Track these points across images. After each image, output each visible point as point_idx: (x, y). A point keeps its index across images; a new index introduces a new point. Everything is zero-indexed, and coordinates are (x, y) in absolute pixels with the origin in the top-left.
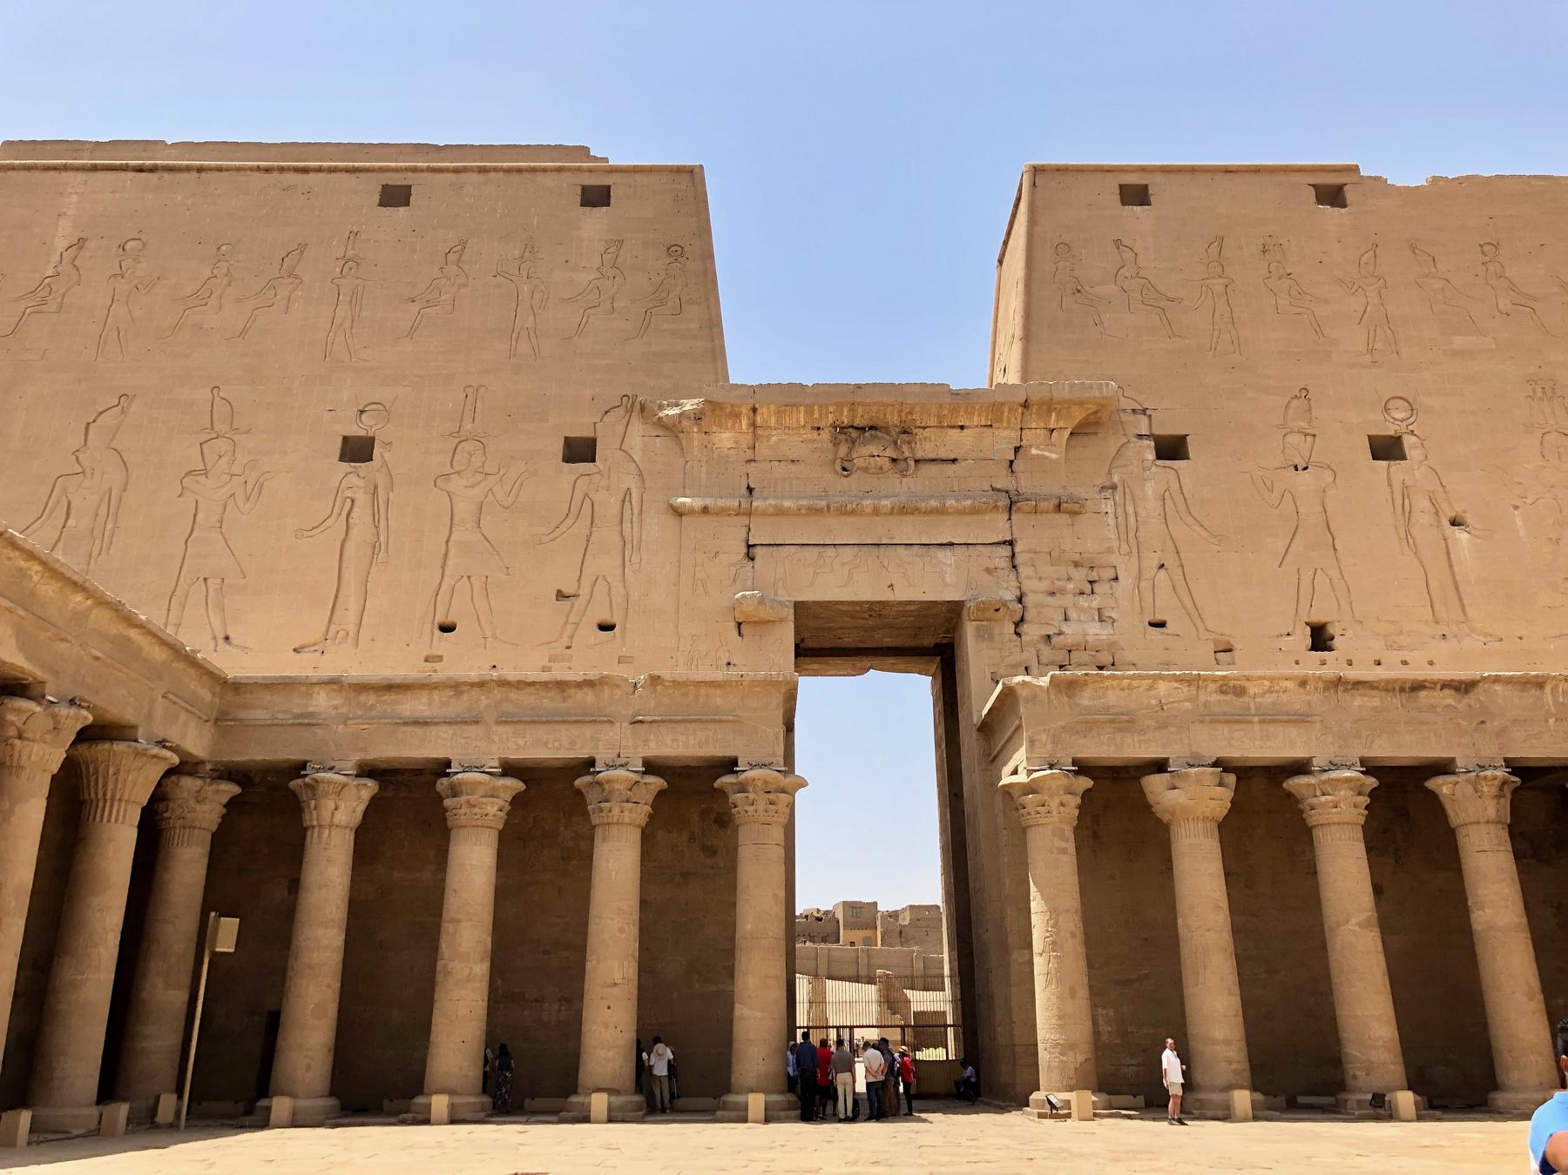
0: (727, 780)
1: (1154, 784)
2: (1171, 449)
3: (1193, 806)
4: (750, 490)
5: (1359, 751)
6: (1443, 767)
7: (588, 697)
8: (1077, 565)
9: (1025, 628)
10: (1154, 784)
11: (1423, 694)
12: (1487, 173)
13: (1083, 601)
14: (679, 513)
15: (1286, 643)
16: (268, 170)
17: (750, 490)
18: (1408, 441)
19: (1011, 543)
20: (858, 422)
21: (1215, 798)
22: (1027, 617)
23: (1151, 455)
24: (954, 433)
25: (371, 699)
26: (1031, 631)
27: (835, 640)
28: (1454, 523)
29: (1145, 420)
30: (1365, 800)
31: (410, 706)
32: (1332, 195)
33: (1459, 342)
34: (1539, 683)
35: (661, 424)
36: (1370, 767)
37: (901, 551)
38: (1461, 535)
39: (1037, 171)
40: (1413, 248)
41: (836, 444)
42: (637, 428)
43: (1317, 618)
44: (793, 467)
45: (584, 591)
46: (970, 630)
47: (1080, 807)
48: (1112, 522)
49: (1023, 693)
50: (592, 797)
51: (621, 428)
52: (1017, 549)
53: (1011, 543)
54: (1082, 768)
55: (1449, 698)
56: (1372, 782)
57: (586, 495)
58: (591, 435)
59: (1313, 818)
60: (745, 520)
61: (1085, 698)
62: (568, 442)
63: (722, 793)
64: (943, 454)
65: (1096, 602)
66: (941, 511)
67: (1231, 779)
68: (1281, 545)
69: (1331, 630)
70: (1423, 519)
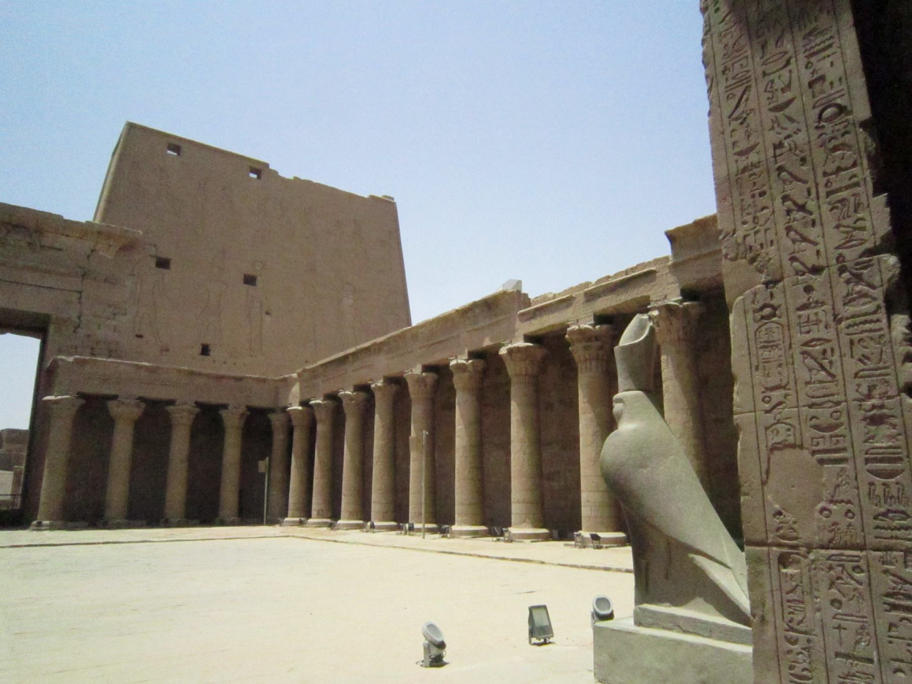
2: (163, 263)
3: (125, 414)
5: (195, 398)
6: (225, 406)
8: (109, 306)
9: (79, 330)
11: (224, 380)
12: (315, 181)
13: (108, 322)
18: (259, 279)
19: (80, 292)
21: (136, 412)
23: (153, 265)
24: (63, 238)
26: (82, 332)
28: (267, 313)
30: (192, 417)
32: (257, 172)
34: (264, 381)
36: (198, 404)
38: (268, 318)
39: (132, 128)
49: (60, 363)
53: (80, 292)
54: (81, 395)
61: (87, 368)
65: (114, 323)
66: (48, 272)
67: (143, 405)
69: (212, 348)
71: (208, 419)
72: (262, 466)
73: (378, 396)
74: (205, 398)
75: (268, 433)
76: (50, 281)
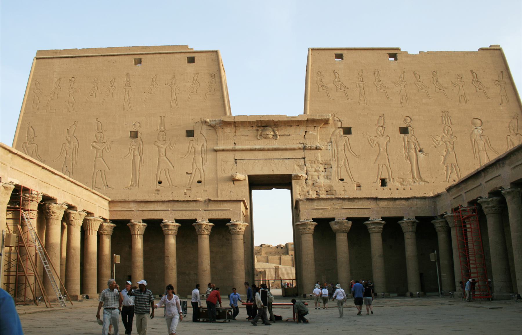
0: (228, 224)
1: (332, 223)
2: (347, 131)
4: (235, 144)
6: (401, 218)
7: (194, 204)
9: (308, 181)
10: (332, 223)
14: (216, 151)
15: (374, 184)
16: (104, 56)
17: (235, 144)
18: (409, 128)
19: (304, 158)
20: (263, 125)
22: (308, 178)
23: (342, 133)
24: (289, 128)
25: (143, 205)
27: (258, 182)
28: (420, 151)
29: (340, 123)
30: (382, 227)
31: (152, 207)
33: (424, 101)
35: (210, 126)
37: (275, 160)
40: (414, 73)
41: (257, 130)
42: (205, 127)
43: (383, 177)
44: (246, 137)
45: (194, 172)
46: (294, 182)
47: (315, 230)
48: (330, 151)
50: (196, 227)
51: (200, 127)
52: (306, 160)
55: (404, 202)
56: (383, 222)
57: (192, 146)
58: (192, 129)
59: (370, 231)
60: (234, 152)
62: (187, 131)
63: (228, 226)
64: (286, 133)
68: (375, 158)
70: (413, 151)
71: (392, 226)
72: (432, 257)
73: (508, 199)
74: (387, 215)
75: (434, 235)
76: (287, 154)
